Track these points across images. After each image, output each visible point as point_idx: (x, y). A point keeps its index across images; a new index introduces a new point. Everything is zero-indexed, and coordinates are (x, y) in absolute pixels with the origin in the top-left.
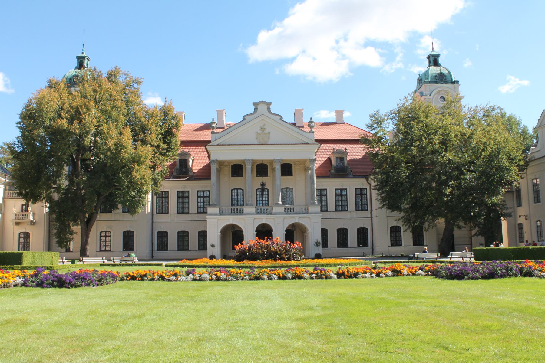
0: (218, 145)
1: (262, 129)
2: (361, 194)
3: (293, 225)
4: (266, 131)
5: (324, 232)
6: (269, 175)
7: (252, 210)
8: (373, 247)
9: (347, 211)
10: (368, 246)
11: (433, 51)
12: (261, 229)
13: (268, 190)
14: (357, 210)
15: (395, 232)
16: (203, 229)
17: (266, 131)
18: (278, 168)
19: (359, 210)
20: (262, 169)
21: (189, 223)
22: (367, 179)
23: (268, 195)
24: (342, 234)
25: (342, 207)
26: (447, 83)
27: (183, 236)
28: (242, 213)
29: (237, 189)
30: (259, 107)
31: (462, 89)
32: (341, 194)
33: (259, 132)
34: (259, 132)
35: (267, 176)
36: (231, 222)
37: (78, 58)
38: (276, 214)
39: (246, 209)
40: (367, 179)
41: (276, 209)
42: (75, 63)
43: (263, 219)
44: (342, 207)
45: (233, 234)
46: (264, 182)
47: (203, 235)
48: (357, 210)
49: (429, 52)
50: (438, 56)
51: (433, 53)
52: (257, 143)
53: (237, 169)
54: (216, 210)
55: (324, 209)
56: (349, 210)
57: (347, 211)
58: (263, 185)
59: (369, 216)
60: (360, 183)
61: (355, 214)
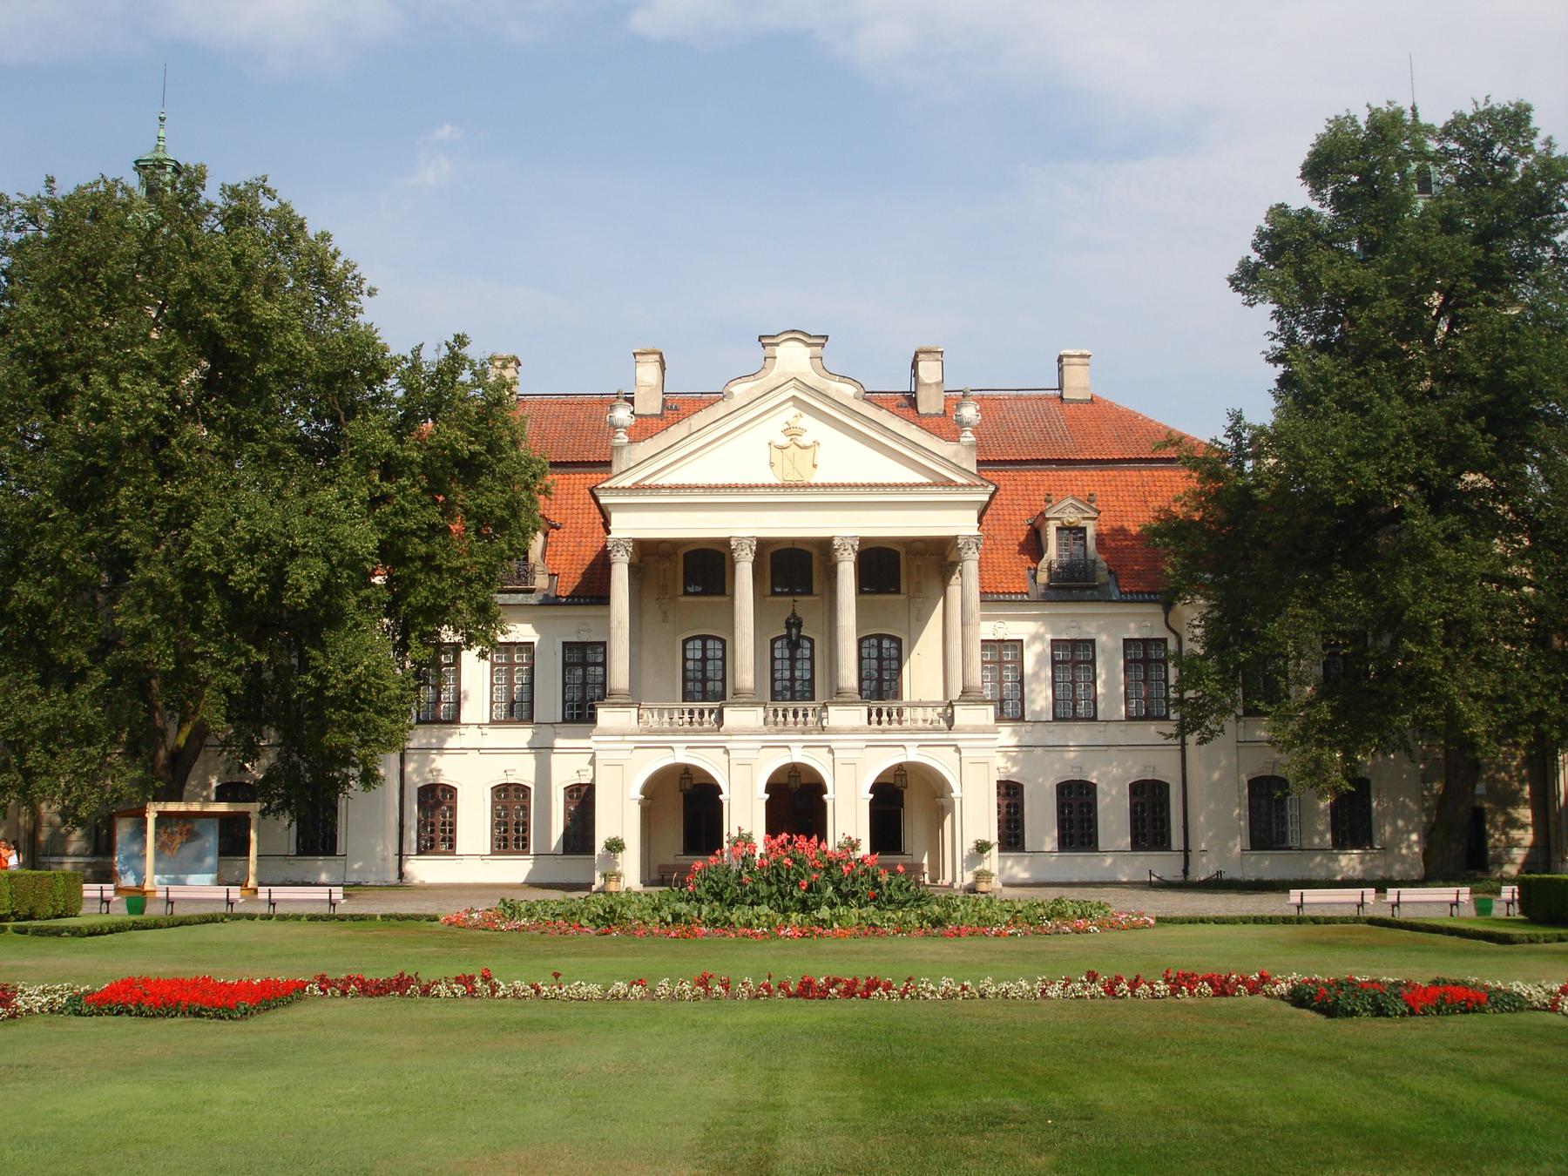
0: (637, 488)
1: (791, 432)
2: (1146, 661)
3: (900, 770)
5: (1010, 793)
6: (816, 589)
8: (1186, 850)
9: (1094, 719)
10: (1168, 848)
12: (784, 780)
13: (811, 641)
14: (1129, 718)
17: (805, 440)
19: (1138, 718)
22: (1168, 607)
23: (812, 659)
24: (1077, 806)
29: (704, 639)
32: (1072, 658)
33: (785, 441)
34: (785, 441)
35: (809, 592)
36: (682, 756)
38: (836, 731)
39: (732, 716)
40: (1168, 607)
41: (838, 716)
46: (799, 614)
47: (582, 799)
48: (1129, 718)
52: (773, 481)
53: (704, 566)
55: (1010, 709)
56: (1100, 717)
57: (1094, 719)
58: (794, 623)
60: (1141, 622)
61: (1117, 734)
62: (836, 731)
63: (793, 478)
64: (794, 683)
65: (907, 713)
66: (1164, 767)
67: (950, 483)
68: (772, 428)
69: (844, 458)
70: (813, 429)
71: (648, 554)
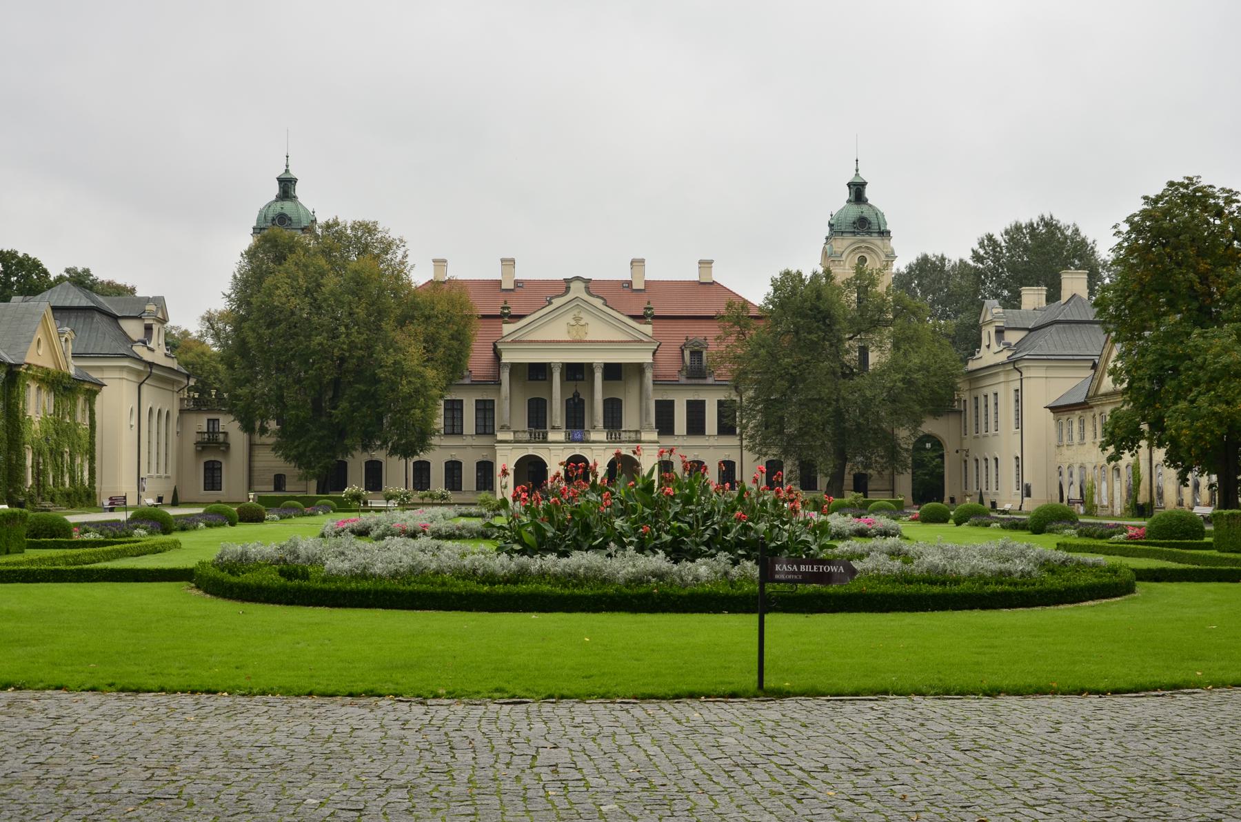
0: (514, 341)
1: (577, 319)
4: (582, 322)
7: (561, 436)
11: (857, 175)
15: (773, 468)
16: (489, 459)
17: (582, 322)
18: (598, 376)
20: (576, 373)
21: (468, 452)
25: (696, 426)
26: (869, 233)
27: (453, 469)
28: (545, 440)
30: (572, 285)
31: (895, 243)
34: (573, 322)
36: (531, 452)
37: (280, 180)
38: (594, 442)
39: (552, 436)
41: (594, 436)
42: (275, 190)
43: (578, 449)
44: (696, 426)
45: (531, 471)
49: (850, 177)
50: (864, 184)
51: (858, 180)
53: (539, 371)
54: (509, 436)
59: (738, 443)
62: (594, 442)
63: (578, 338)
64: (576, 420)
65: (623, 435)
66: (734, 456)
67: (641, 341)
68: (569, 318)
69: (597, 330)
70: (586, 318)
71: (515, 368)
